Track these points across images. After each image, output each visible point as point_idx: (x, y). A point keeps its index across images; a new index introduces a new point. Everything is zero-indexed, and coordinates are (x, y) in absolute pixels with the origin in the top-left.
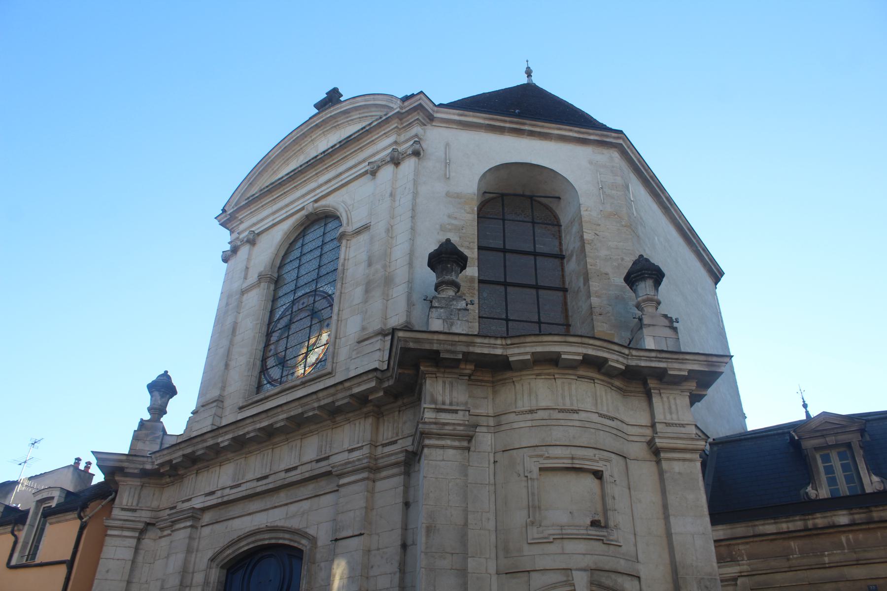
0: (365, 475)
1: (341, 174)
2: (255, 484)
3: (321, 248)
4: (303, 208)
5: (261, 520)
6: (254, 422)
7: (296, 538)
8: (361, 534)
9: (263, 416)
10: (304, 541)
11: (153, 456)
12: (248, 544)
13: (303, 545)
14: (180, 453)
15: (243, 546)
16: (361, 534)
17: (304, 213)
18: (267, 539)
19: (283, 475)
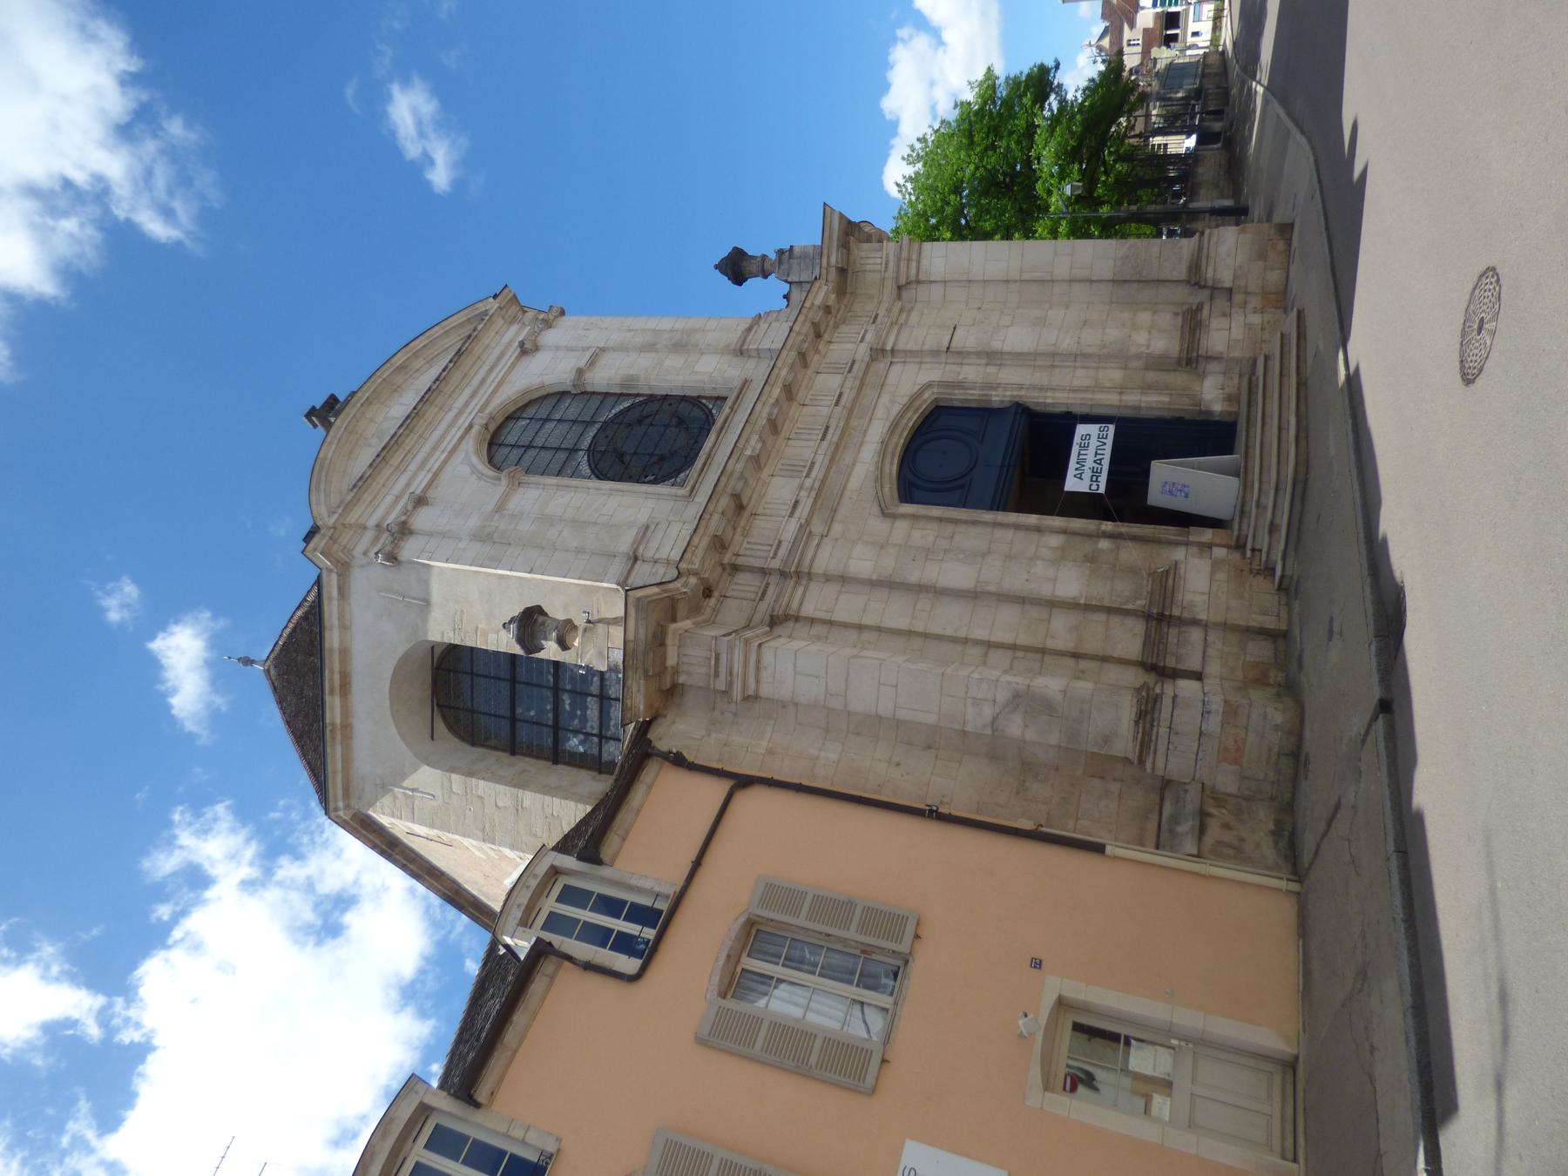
0: (895, 329)
1: (483, 381)
2: (825, 444)
3: (525, 451)
4: (470, 426)
5: (876, 432)
6: (764, 404)
7: (916, 404)
8: (955, 328)
9: (767, 388)
10: (926, 395)
11: (683, 566)
12: (892, 464)
13: (929, 397)
14: (716, 517)
15: (891, 470)
16: (955, 328)
17: (476, 428)
18: (899, 441)
19: (838, 409)
